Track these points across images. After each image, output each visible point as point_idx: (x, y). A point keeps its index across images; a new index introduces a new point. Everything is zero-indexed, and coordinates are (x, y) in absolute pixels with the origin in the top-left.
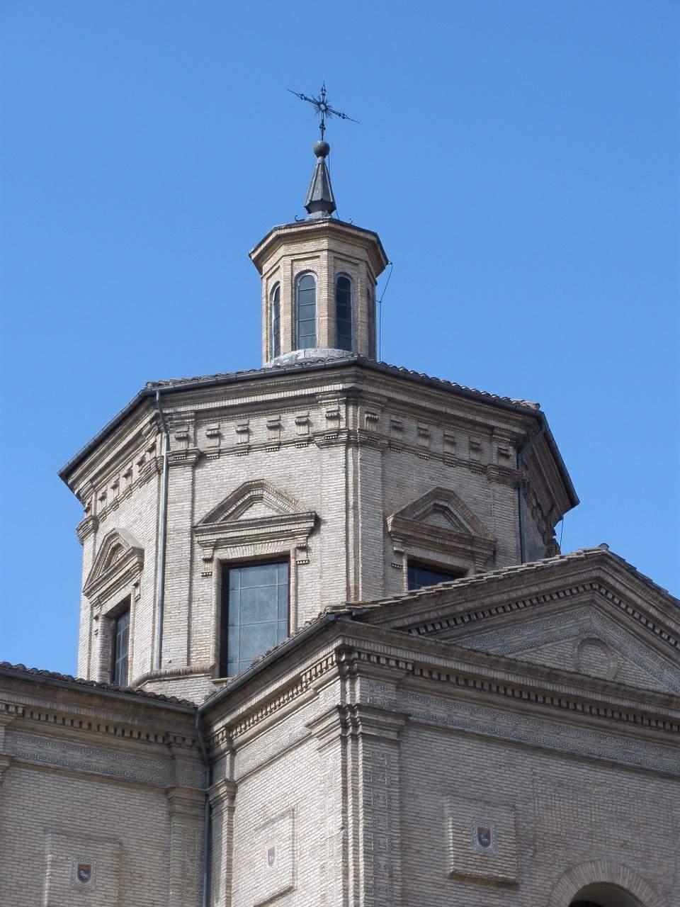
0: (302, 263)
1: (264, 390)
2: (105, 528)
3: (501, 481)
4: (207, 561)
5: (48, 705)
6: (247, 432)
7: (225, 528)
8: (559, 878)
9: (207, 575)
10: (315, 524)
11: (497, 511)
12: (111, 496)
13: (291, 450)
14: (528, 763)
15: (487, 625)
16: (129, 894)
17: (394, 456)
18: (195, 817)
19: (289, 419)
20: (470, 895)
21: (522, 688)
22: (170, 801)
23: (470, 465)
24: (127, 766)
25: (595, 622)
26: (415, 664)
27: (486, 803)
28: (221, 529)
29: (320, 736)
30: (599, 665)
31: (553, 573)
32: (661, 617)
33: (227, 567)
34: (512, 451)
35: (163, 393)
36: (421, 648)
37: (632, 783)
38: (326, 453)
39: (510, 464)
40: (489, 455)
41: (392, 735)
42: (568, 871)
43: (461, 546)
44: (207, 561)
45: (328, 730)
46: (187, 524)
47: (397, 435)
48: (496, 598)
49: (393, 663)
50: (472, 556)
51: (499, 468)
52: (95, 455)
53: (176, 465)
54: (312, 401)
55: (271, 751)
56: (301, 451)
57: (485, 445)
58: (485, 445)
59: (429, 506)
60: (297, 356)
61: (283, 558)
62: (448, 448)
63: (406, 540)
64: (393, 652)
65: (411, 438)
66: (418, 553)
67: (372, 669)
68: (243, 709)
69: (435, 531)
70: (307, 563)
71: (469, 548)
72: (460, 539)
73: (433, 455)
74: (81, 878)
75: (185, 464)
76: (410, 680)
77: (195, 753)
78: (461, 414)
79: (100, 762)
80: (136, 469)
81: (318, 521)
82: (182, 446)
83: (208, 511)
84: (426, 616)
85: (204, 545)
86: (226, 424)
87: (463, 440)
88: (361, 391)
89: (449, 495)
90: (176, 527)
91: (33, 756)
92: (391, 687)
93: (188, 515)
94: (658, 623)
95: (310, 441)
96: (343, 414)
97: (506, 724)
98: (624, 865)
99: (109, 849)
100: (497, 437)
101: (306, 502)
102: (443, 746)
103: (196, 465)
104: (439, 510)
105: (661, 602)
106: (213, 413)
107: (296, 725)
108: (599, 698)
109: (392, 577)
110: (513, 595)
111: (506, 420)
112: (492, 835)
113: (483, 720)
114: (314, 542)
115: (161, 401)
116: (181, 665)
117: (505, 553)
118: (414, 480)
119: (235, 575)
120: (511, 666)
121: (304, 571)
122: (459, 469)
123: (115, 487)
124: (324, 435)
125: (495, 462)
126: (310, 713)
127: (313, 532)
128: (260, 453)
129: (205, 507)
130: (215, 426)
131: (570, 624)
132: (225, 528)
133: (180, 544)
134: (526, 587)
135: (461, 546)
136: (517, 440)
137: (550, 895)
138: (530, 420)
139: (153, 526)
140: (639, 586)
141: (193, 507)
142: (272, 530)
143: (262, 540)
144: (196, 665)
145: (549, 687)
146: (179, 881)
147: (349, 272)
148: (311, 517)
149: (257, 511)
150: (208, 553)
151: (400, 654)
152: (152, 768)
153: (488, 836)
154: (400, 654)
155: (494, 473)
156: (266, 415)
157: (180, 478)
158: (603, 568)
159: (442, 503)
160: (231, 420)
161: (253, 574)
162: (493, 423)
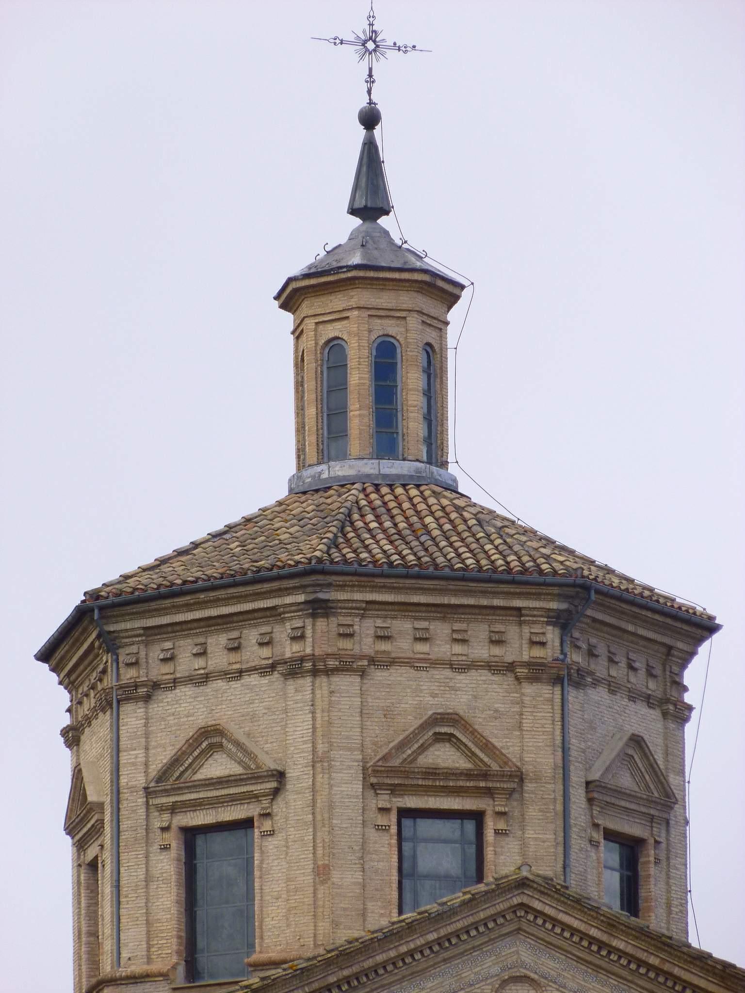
0: (329, 327)
1: (216, 602)
3: (534, 679)
4: (165, 829)
6: (203, 654)
7: (180, 788)
9: (165, 848)
10: (280, 782)
13: (253, 680)
15: (374, 987)
17: (379, 675)
19: (251, 636)
32: (604, 938)
35: (101, 609)
38: (291, 685)
40: (517, 648)
43: (472, 784)
46: (140, 780)
47: (384, 646)
48: (380, 958)
50: (489, 792)
53: (128, 699)
54: (273, 614)
56: (265, 681)
59: (426, 737)
60: (320, 473)
61: (247, 824)
62: (458, 649)
63: (394, 790)
65: (403, 646)
66: (412, 802)
69: (432, 773)
70: (272, 833)
71: (482, 784)
72: (468, 775)
73: (435, 663)
75: (136, 699)
78: (471, 601)
81: (280, 776)
82: (129, 675)
83: (165, 761)
85: (161, 809)
87: (479, 631)
89: (453, 719)
90: (130, 784)
93: (142, 768)
95: (273, 667)
96: (309, 632)
100: (527, 618)
103: (147, 698)
104: (440, 738)
105: (602, 921)
106: (165, 630)
109: (375, 843)
110: (404, 949)
111: (537, 596)
114: (279, 807)
115: (101, 617)
116: (137, 968)
117: (537, 779)
119: (200, 841)
121: (271, 844)
122: (473, 673)
124: (286, 663)
125: (526, 658)
128: (220, 684)
129: (161, 758)
130: (168, 645)
131: (488, 962)
132: (180, 788)
133: (134, 803)
134: (422, 936)
135: (472, 784)
136: (558, 617)
140: (573, 907)
141: (147, 756)
142: (232, 791)
143: (223, 802)
144: (154, 968)
147: (392, 331)
148: (273, 775)
149: (218, 767)
155: (522, 671)
156: (227, 630)
157: (132, 717)
158: (526, 892)
159: (444, 730)
160: (187, 636)
162: (518, 603)
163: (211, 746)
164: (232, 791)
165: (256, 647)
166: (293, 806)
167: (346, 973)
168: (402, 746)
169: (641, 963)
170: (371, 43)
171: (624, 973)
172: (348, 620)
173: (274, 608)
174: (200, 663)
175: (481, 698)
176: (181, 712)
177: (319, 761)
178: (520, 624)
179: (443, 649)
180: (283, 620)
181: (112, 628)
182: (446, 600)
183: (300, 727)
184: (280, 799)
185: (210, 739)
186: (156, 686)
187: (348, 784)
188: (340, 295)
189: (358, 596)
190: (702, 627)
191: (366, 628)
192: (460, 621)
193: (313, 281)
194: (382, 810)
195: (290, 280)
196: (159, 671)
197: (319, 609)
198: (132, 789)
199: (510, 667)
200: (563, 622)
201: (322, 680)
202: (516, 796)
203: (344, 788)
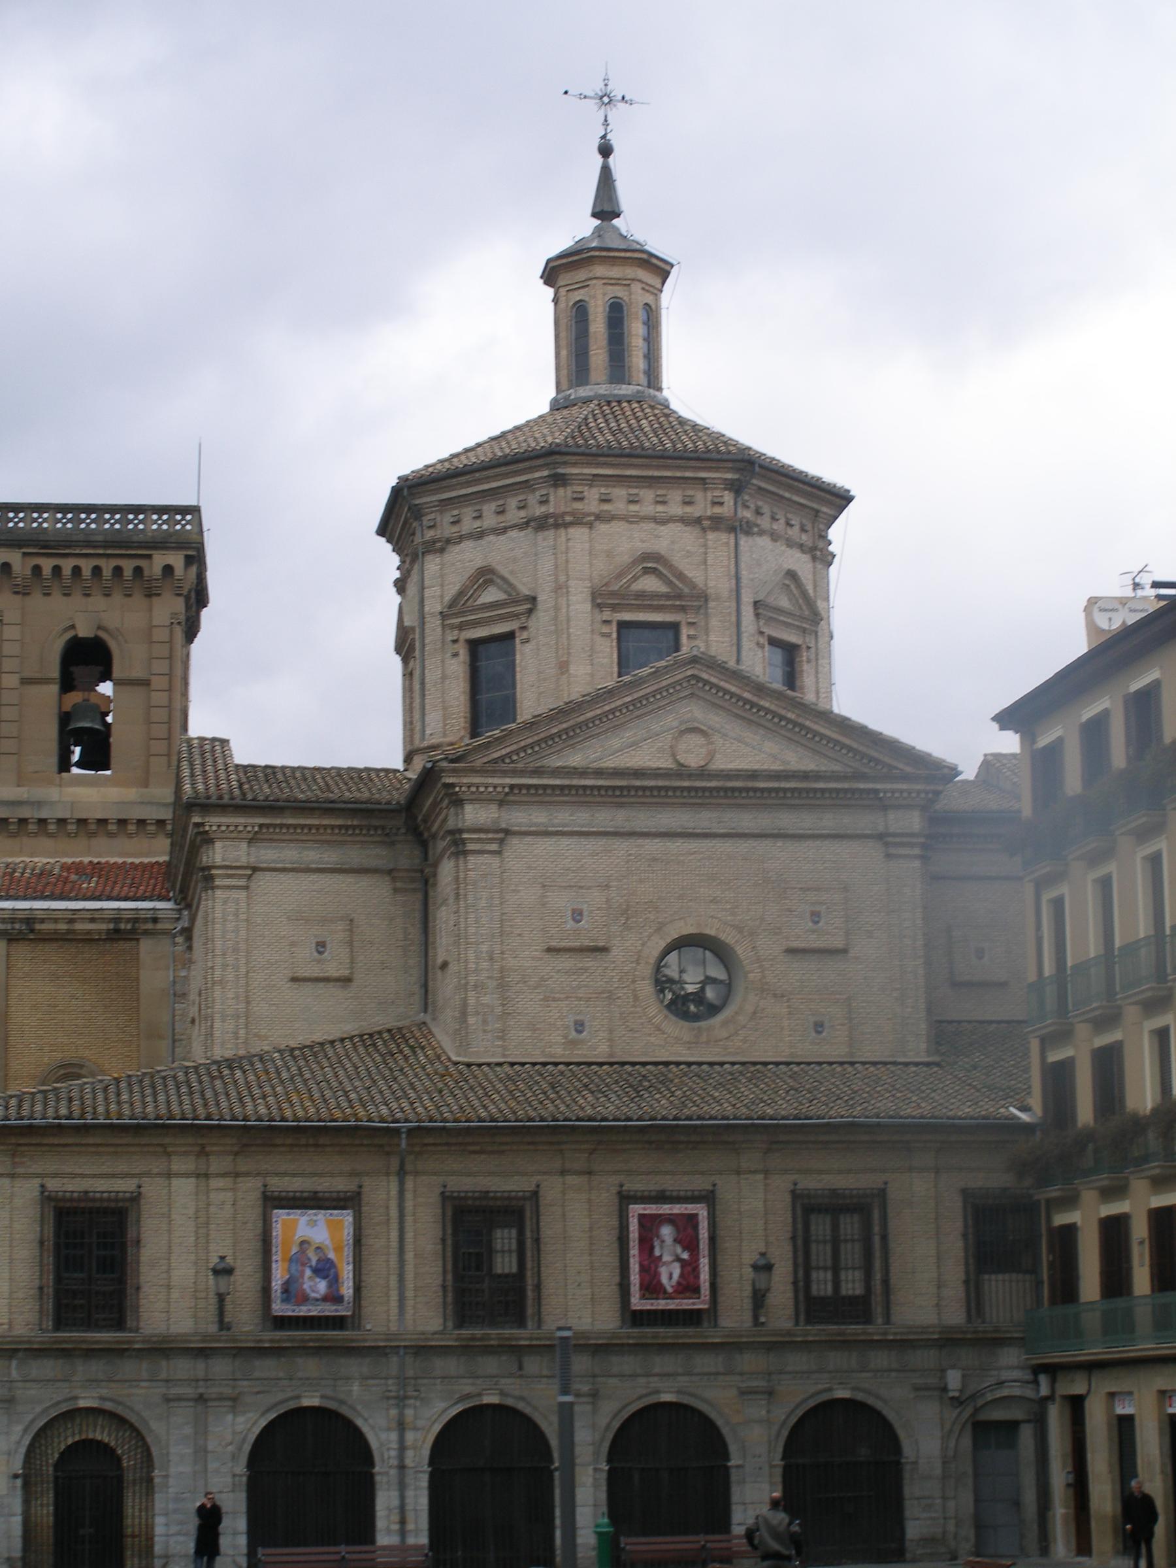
0: (576, 293)
1: (488, 479)
4: (455, 641)
5: (278, 821)
6: (479, 517)
8: (649, 937)
9: (455, 655)
13: (514, 534)
14: (622, 847)
16: (361, 958)
17: (603, 527)
18: (414, 890)
19: (513, 502)
20: (566, 962)
22: (394, 880)
23: (684, 520)
24: (356, 855)
25: (696, 712)
26: (512, 787)
27: (581, 887)
30: (693, 754)
31: (645, 682)
32: (755, 699)
33: (474, 646)
34: (728, 497)
35: (410, 487)
36: (515, 773)
37: (727, 846)
39: (726, 510)
40: (701, 507)
41: (494, 847)
42: (658, 930)
43: (670, 603)
44: (455, 641)
46: (438, 608)
48: (589, 715)
49: (491, 789)
50: (683, 609)
53: (429, 552)
54: (527, 486)
56: (522, 534)
57: (699, 496)
61: (511, 636)
62: (660, 508)
63: (614, 608)
64: (490, 780)
66: (628, 616)
67: (473, 797)
69: (641, 595)
70: (527, 641)
71: (678, 603)
72: (667, 596)
73: (644, 519)
74: (320, 953)
75: (435, 551)
76: (511, 798)
77: (410, 838)
78: (669, 474)
79: (330, 857)
81: (533, 599)
82: (429, 534)
84: (523, 744)
85: (453, 627)
86: (465, 510)
87: (675, 496)
88: (564, 475)
91: (274, 861)
92: (494, 807)
95: (527, 524)
96: (552, 498)
97: (605, 818)
98: (712, 917)
99: (341, 926)
103: (442, 550)
104: (647, 571)
108: (686, 784)
110: (607, 708)
111: (717, 469)
112: (585, 913)
113: (580, 818)
114: (532, 623)
115: (411, 494)
117: (717, 599)
120: (599, 773)
121: (528, 648)
122: (671, 525)
125: (709, 513)
128: (491, 538)
129: (451, 591)
130: (455, 512)
131: (670, 718)
133: (434, 625)
135: (670, 603)
136: (732, 484)
137: (640, 951)
141: (442, 591)
146: (401, 943)
149: (491, 595)
150: (455, 634)
151: (496, 781)
152: (374, 855)
153: (581, 914)
154: (496, 781)
155: (706, 523)
156: (494, 500)
159: (649, 565)
160: (468, 506)
161: (493, 647)
163: (486, 582)
164: (500, 612)
165: (515, 511)
166: (541, 620)
167: (564, 726)
168: (620, 576)
169: (782, 718)
170: (606, 99)
171: (769, 725)
172: (579, 489)
173: (527, 481)
174: (477, 524)
175: (678, 544)
176: (465, 558)
178: (705, 490)
179: (648, 508)
180: (534, 490)
181: (417, 502)
182: (650, 473)
183: (546, 565)
185: (485, 576)
186: (448, 541)
187: (579, 605)
188: (583, 270)
189: (587, 471)
190: (840, 499)
191: (593, 494)
192: (660, 488)
193: (564, 261)
194: (605, 622)
195: (549, 261)
196: (449, 531)
197: (559, 480)
199: (698, 521)
200: (737, 488)
201: (562, 531)
202: (702, 611)
203: (578, 607)
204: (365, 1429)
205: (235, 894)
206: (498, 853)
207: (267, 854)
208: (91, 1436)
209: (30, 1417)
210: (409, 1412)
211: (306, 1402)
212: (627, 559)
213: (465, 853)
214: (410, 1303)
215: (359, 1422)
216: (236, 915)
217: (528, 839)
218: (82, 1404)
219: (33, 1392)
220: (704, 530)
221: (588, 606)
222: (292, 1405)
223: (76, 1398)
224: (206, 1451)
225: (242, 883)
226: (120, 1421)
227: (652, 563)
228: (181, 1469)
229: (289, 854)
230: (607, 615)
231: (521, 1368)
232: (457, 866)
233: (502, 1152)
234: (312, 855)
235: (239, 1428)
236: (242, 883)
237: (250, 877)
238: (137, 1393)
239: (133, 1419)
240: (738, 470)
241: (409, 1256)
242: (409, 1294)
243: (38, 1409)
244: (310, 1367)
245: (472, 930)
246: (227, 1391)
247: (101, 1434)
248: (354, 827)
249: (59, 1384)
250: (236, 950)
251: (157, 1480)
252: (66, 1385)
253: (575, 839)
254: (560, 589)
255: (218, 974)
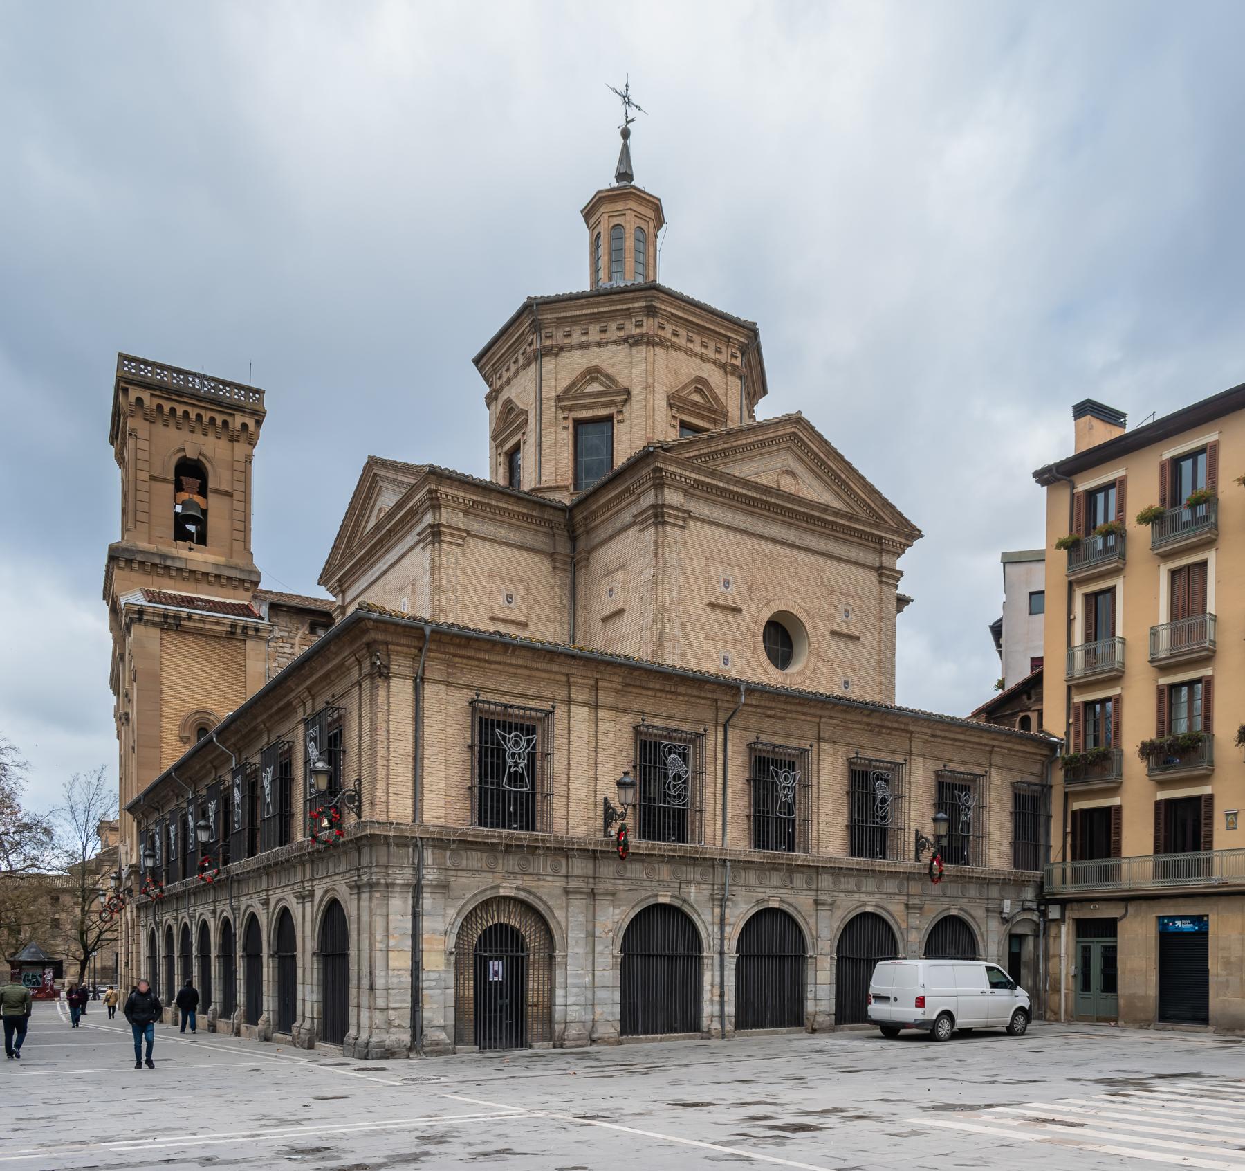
2: (503, 396)
3: (733, 374)
4: (565, 418)
9: (566, 428)
11: (730, 392)
12: (506, 376)
21: (751, 497)
23: (716, 363)
28: (574, 398)
29: (641, 523)
33: (578, 423)
34: (739, 355)
39: (738, 362)
41: (681, 523)
44: (565, 418)
45: (646, 520)
46: (553, 395)
51: (732, 365)
52: (495, 348)
55: (610, 532)
57: (724, 350)
58: (724, 350)
61: (610, 419)
62: (704, 351)
68: (594, 507)
69: (695, 404)
70: (622, 422)
73: (695, 355)
79: (515, 537)
80: (521, 359)
87: (712, 345)
94: (823, 462)
97: (741, 520)
101: (623, 381)
102: (707, 530)
107: (627, 517)
113: (727, 516)
114: (626, 409)
118: (684, 370)
120: (746, 483)
121: (622, 426)
123: (507, 370)
126: (634, 510)
127: (626, 401)
133: (549, 407)
138: (751, 334)
139: (533, 395)
145: (765, 498)
149: (595, 387)
150: (566, 414)
162: (730, 334)
166: (636, 405)
168: (684, 387)
177: (650, 387)
179: (697, 349)
184: (628, 406)
187: (661, 403)
198: (548, 399)
204: (698, 923)
205: (455, 549)
206: (683, 528)
207: (475, 526)
208: (506, 921)
209: (463, 902)
210: (727, 911)
211: (661, 900)
212: (685, 380)
213: (664, 523)
214: (729, 827)
215: (695, 917)
216: (456, 564)
217: (699, 524)
218: (502, 892)
219: (464, 880)
220: (726, 373)
221: (664, 404)
222: (652, 901)
223: (498, 887)
224: (594, 936)
225: (460, 542)
226: (528, 908)
227: (701, 384)
228: (577, 950)
229: (489, 529)
230: (674, 413)
231: (792, 882)
232: (656, 533)
233: (783, 719)
234: (503, 533)
235: (614, 918)
236: (460, 542)
237: (464, 538)
238: (544, 886)
239: (541, 907)
240: (748, 337)
241: (729, 790)
242: (729, 820)
243: (468, 896)
244: (664, 872)
245: (668, 580)
246: (610, 887)
247: (512, 920)
248: (532, 516)
249: (484, 875)
250: (455, 590)
251: (558, 959)
252: (490, 875)
253: (724, 530)
254: (650, 387)
255: (443, 605)
